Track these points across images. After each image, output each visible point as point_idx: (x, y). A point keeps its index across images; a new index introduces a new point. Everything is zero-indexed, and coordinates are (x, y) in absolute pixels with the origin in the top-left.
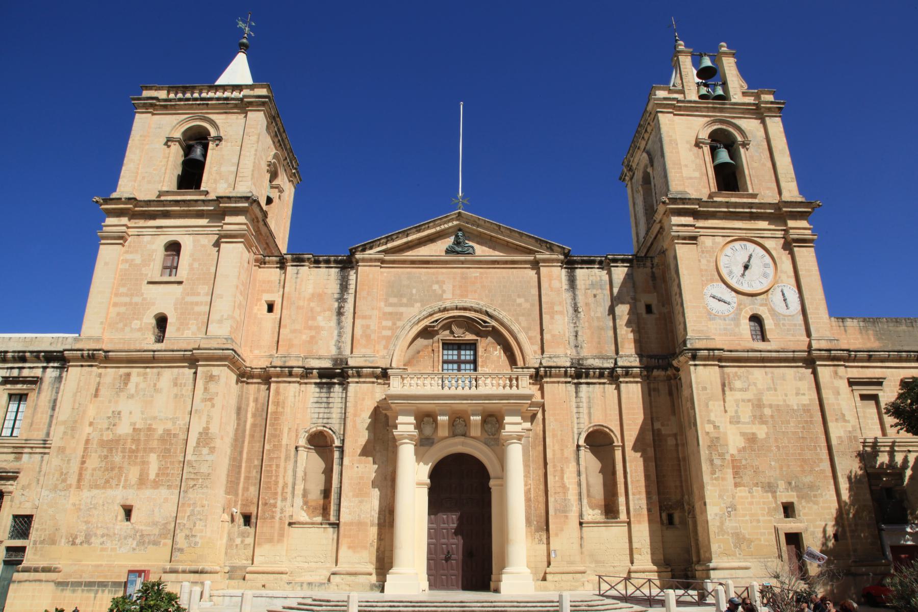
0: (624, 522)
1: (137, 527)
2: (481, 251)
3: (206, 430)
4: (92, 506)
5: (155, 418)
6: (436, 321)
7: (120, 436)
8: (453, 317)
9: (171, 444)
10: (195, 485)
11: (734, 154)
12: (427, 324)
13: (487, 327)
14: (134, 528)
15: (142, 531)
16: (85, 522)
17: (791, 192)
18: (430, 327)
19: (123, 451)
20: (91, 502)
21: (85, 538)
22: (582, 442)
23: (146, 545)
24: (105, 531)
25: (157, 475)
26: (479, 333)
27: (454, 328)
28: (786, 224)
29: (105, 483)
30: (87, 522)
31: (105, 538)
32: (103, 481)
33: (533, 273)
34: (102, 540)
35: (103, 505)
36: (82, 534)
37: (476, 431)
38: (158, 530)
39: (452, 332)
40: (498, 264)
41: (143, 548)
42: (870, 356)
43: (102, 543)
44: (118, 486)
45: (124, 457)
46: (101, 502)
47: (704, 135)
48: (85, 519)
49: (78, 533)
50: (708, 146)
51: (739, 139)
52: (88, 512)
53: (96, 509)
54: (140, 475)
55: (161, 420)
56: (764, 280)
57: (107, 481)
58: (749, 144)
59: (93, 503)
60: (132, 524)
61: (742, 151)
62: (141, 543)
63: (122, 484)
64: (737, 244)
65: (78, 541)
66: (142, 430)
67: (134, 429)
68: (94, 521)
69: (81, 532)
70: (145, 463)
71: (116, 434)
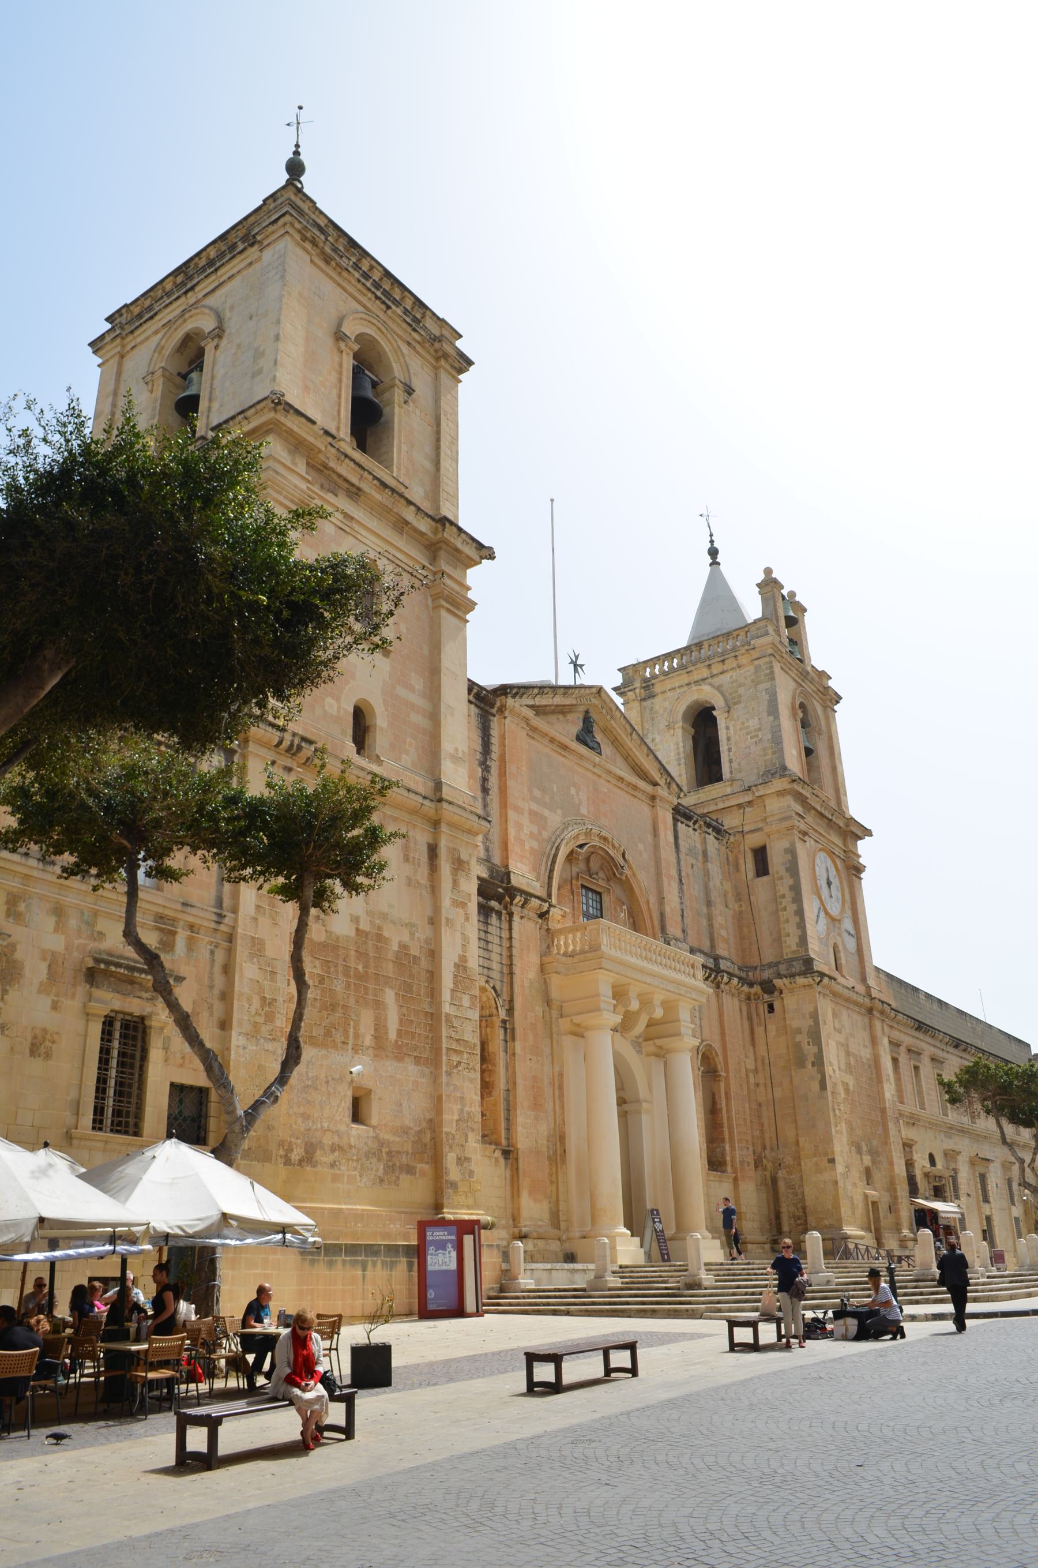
1: (381, 1136)
3: (463, 959)
4: (309, 1083)
5: (384, 916)
7: (338, 938)
9: (411, 976)
10: (459, 1063)
14: (376, 1137)
15: (389, 1142)
16: (302, 1115)
19: (347, 975)
20: (307, 1073)
21: (306, 1151)
23: (397, 1173)
24: (336, 1139)
25: (399, 1033)
29: (325, 1035)
30: (306, 1117)
31: (336, 1154)
32: (322, 1031)
33: (646, 809)
34: (331, 1158)
35: (327, 1082)
36: (299, 1141)
38: (410, 1145)
41: (393, 1178)
43: (333, 1165)
44: (345, 1046)
45: (348, 986)
46: (323, 1076)
48: (302, 1110)
49: (293, 1140)
52: (305, 1095)
53: (316, 1089)
54: (376, 1030)
55: (393, 922)
57: (328, 1034)
59: (310, 1075)
60: (374, 1127)
62: (390, 1168)
63: (351, 1042)
65: (295, 1156)
66: (370, 937)
67: (357, 930)
68: (316, 1115)
69: (298, 1138)
70: (379, 1005)
71: (331, 932)
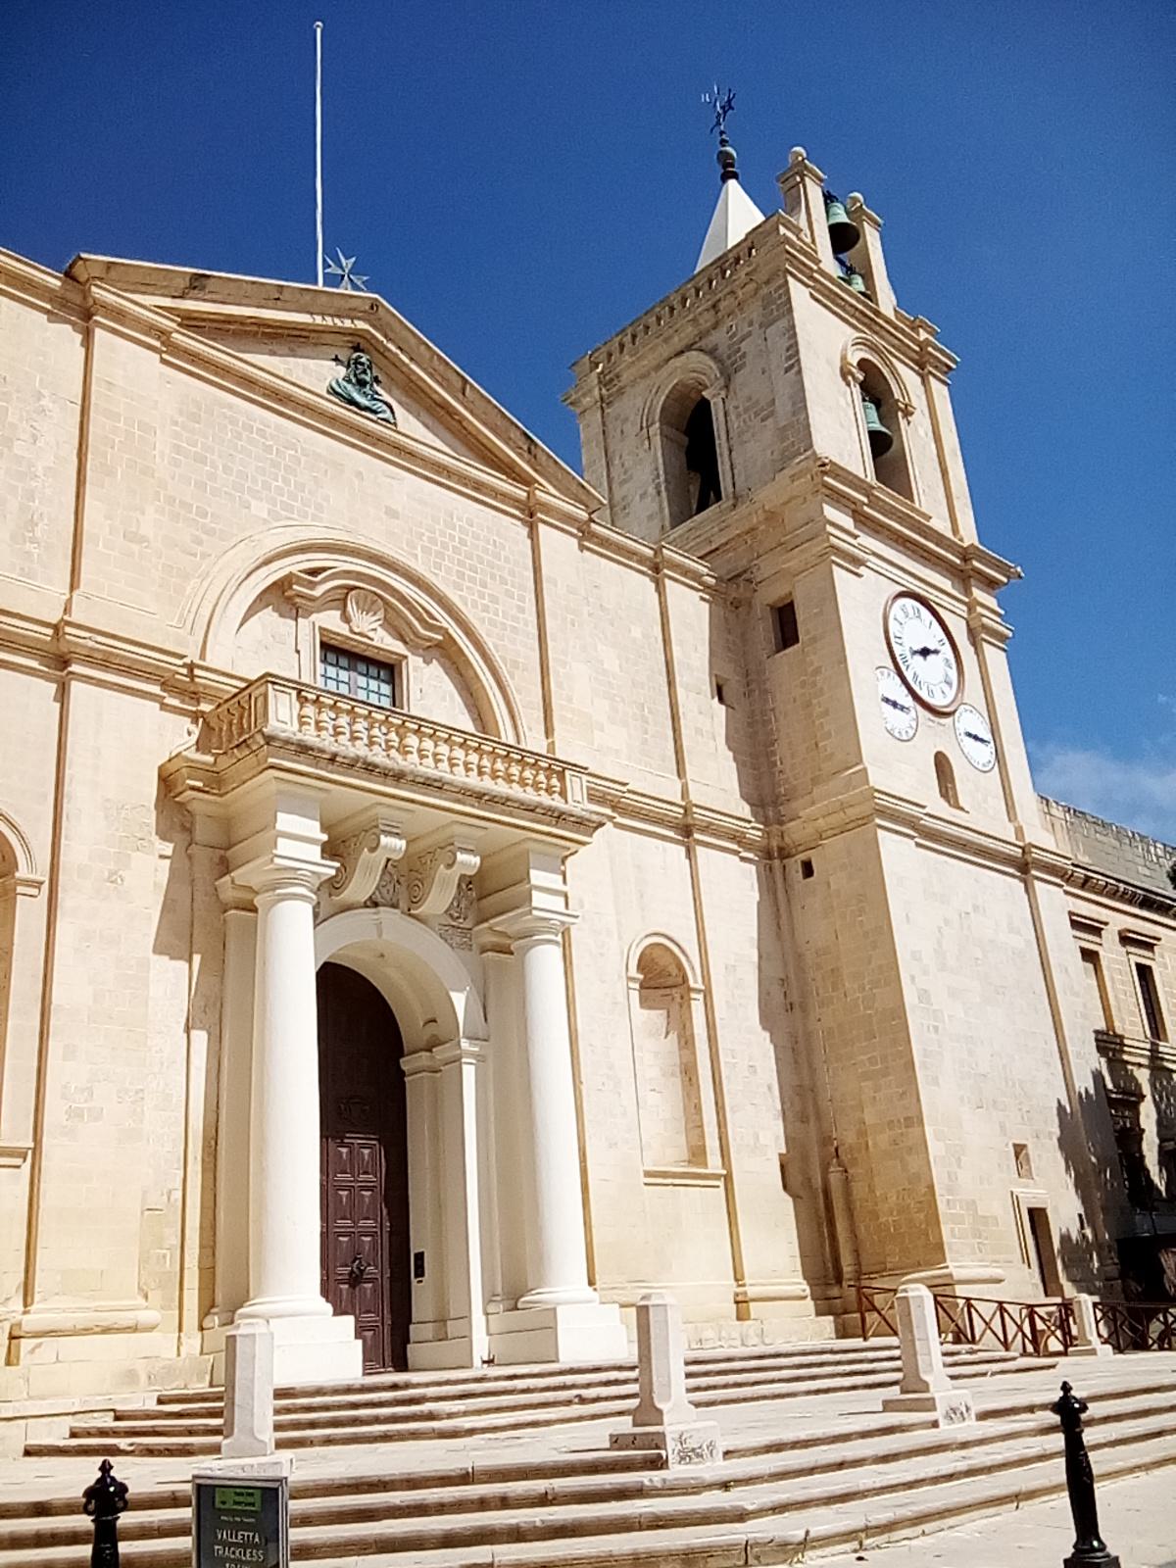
0: (717, 1177)
2: (410, 426)
6: (314, 572)
8: (359, 576)
12: (295, 569)
17: (969, 536)
18: (300, 581)
22: (633, 972)
26: (414, 648)
27: (351, 608)
28: (967, 592)
37: (439, 899)
39: (346, 619)
40: (449, 478)
42: (1087, 879)
47: (854, 359)
56: (946, 688)
58: (912, 414)
61: (903, 423)
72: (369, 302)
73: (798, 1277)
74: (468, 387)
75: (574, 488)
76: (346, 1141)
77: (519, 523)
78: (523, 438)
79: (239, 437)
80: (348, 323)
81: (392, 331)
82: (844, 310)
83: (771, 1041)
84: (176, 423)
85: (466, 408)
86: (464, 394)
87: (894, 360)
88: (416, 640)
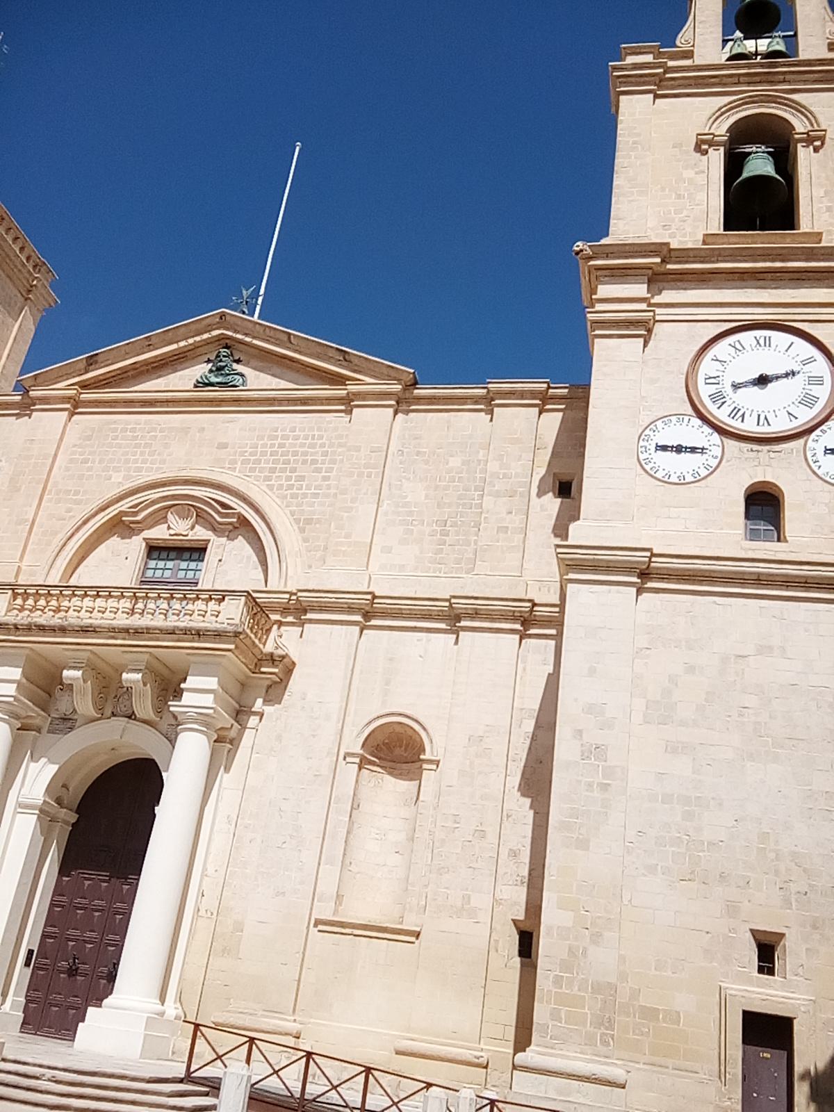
8: (174, 497)
11: (784, 159)
13: (227, 516)
50: (722, 149)
51: (800, 125)
64: (747, 337)
72: (219, 316)
73: (508, 1048)
74: (292, 337)
75: (385, 371)
76: (129, 881)
77: (343, 414)
78: (338, 353)
79: (116, 438)
80: (206, 336)
81: (238, 325)
82: (725, 85)
83: (531, 807)
84: (75, 446)
85: (296, 351)
86: (291, 343)
87: (795, 97)
88: (220, 526)
